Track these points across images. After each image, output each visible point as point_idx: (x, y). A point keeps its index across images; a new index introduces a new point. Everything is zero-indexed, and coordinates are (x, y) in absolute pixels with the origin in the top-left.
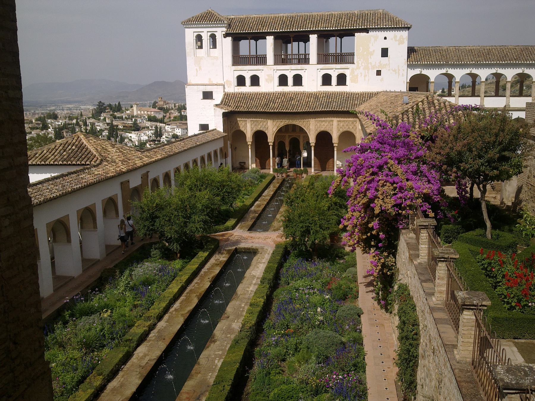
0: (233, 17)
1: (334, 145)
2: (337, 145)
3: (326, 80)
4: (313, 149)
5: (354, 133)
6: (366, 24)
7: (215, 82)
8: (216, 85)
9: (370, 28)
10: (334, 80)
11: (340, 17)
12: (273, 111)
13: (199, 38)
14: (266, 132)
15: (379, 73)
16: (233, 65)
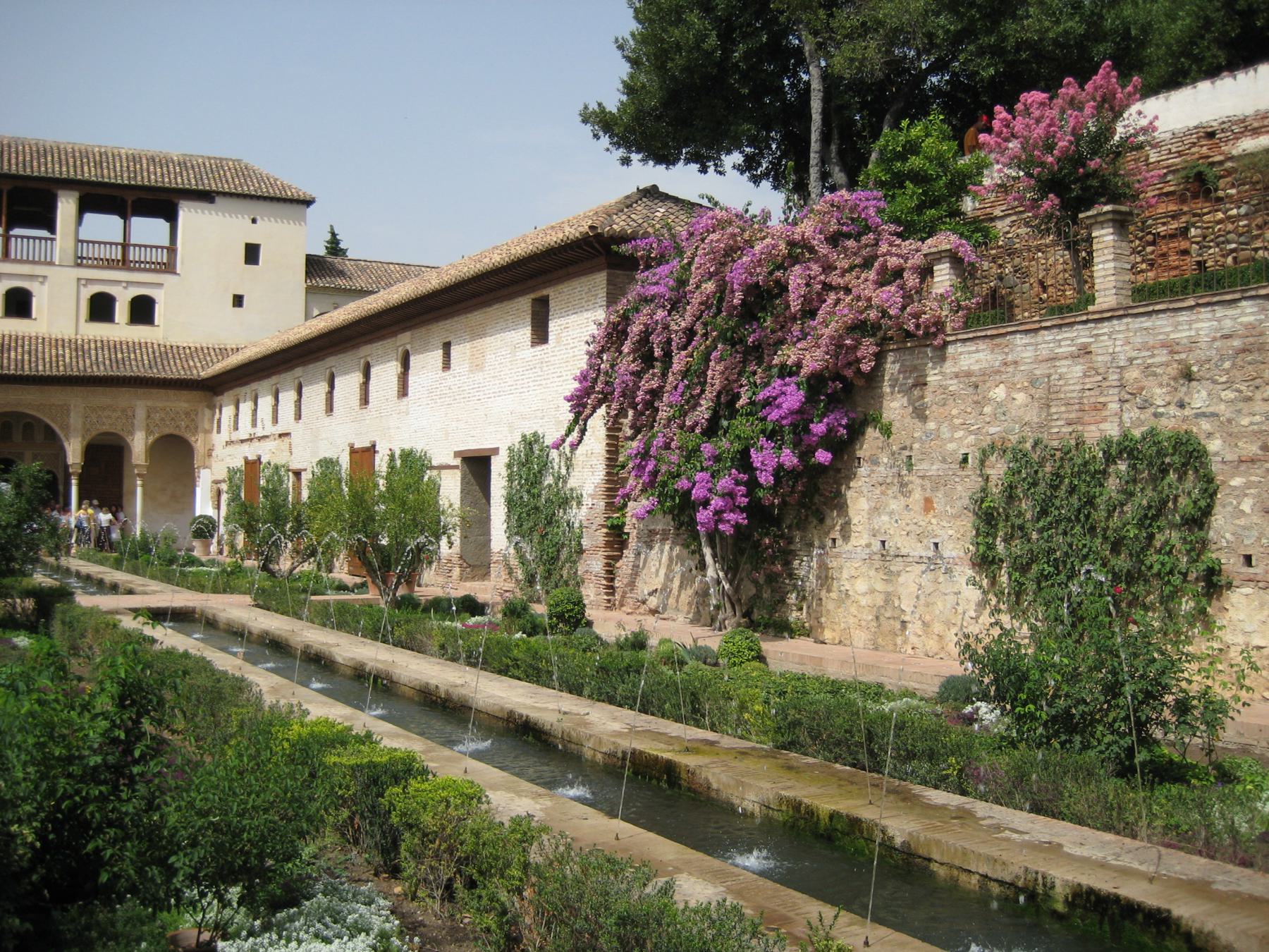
3: (101, 308)
4: (74, 482)
9: (219, 193)
10: (122, 311)
11: (135, 159)
15: (238, 301)
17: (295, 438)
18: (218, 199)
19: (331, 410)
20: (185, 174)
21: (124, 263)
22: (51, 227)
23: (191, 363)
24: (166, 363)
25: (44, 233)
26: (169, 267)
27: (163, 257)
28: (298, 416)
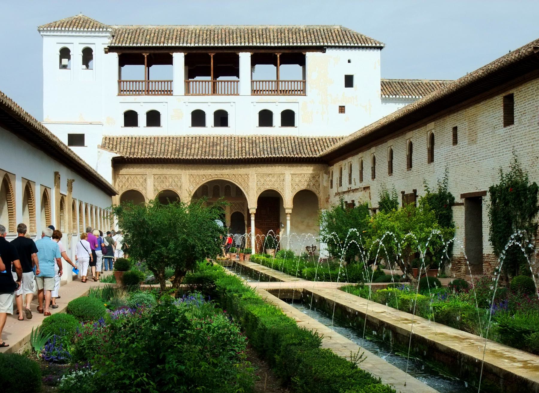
0: (116, 27)
1: (287, 211)
2: (290, 211)
3: (265, 118)
4: (253, 218)
5: (317, 193)
6: (321, 40)
7: (90, 121)
8: (91, 124)
9: (328, 47)
10: (277, 119)
11: (281, 31)
12: (191, 157)
13: (65, 53)
14: (178, 192)
15: (342, 109)
16: (118, 95)
17: (372, 190)
18: (327, 50)
19: (392, 173)
20: (309, 36)
21: (277, 92)
22: (237, 74)
23: (316, 148)
24: (301, 148)
25: (234, 78)
26: (303, 92)
27: (300, 86)
28: (374, 177)
